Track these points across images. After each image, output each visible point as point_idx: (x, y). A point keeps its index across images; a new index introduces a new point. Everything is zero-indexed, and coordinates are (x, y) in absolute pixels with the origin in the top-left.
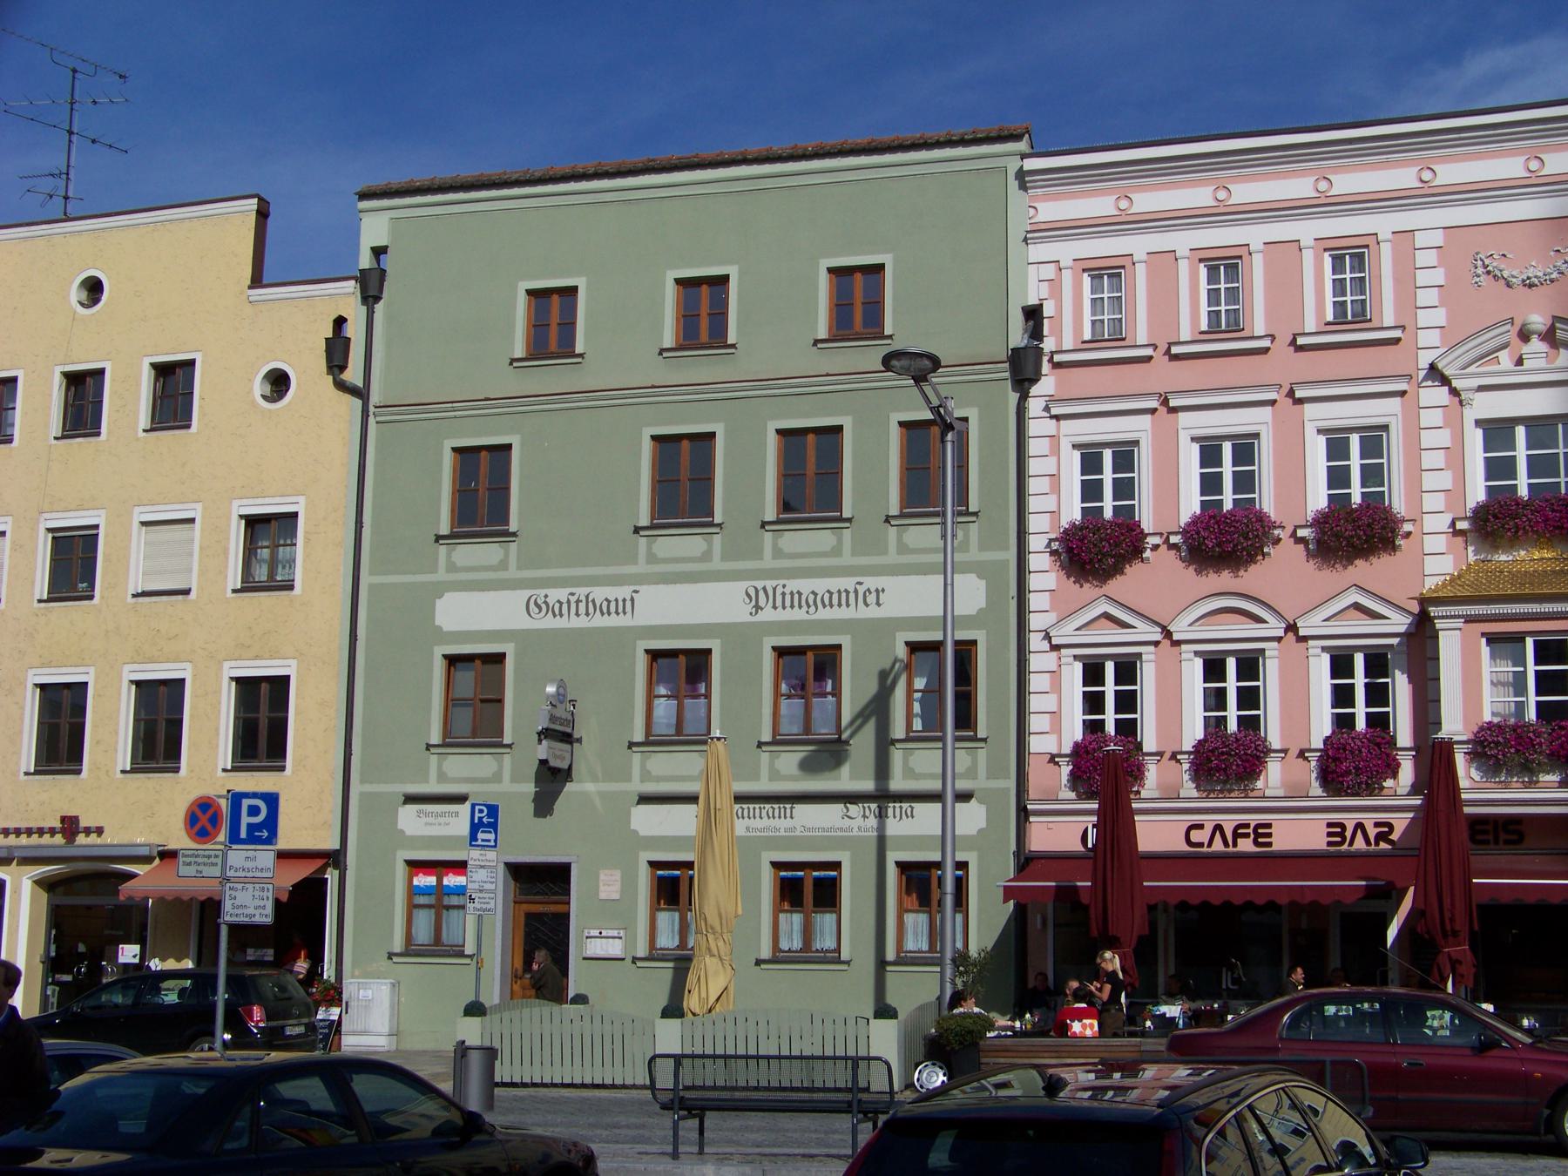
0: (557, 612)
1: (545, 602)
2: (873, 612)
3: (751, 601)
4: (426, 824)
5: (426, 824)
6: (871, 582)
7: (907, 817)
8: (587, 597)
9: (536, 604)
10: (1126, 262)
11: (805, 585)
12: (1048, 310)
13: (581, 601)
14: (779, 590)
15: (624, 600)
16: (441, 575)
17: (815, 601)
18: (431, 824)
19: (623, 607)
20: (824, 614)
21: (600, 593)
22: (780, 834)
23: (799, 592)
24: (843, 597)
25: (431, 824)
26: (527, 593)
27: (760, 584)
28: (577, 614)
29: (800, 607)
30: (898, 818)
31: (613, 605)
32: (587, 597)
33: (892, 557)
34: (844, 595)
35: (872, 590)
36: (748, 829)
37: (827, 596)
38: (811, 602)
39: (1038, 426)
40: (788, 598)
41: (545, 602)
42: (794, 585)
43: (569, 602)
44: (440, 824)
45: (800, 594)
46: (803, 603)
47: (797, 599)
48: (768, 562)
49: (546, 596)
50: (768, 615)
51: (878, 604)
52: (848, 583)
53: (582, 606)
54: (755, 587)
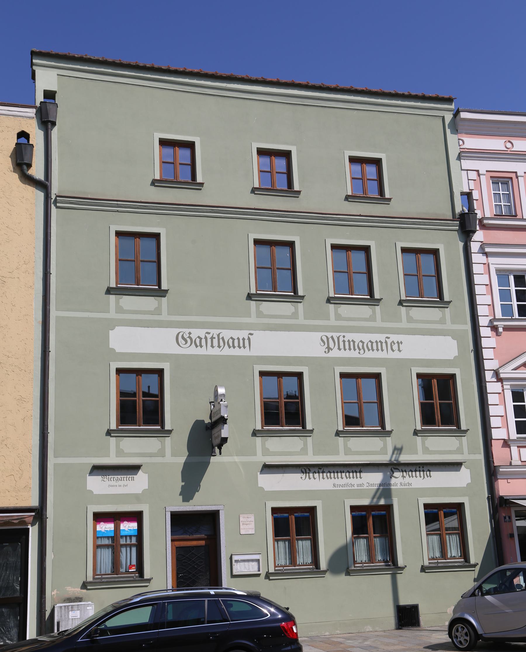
0: (198, 344)
1: (190, 337)
2: (396, 355)
3: (325, 344)
4: (109, 486)
5: (109, 486)
6: (394, 338)
7: (428, 477)
8: (218, 335)
9: (183, 337)
10: (513, 176)
11: (357, 337)
12: (476, 195)
13: (215, 338)
14: (341, 339)
15: (244, 339)
16: (112, 314)
17: (362, 347)
18: (112, 486)
19: (243, 343)
20: (369, 354)
21: (227, 334)
22: (354, 488)
23: (353, 341)
24: (379, 346)
25: (112, 486)
26: (178, 330)
27: (329, 335)
28: (212, 346)
29: (355, 350)
30: (422, 477)
31: (236, 342)
32: (218, 335)
33: (405, 324)
34: (379, 344)
35: (395, 342)
36: (334, 485)
37: (370, 344)
38: (361, 347)
39: (477, 258)
40: (347, 344)
41: (190, 337)
42: (349, 336)
43: (206, 338)
44: (120, 486)
45: (354, 342)
46: (356, 347)
47: (352, 345)
48: (333, 322)
49: (190, 333)
50: (335, 353)
51: (399, 350)
52: (381, 337)
53: (215, 341)
54: (326, 336)
